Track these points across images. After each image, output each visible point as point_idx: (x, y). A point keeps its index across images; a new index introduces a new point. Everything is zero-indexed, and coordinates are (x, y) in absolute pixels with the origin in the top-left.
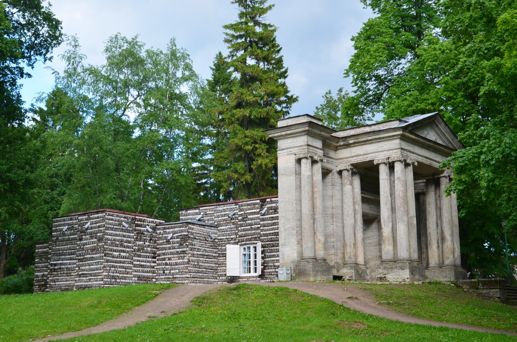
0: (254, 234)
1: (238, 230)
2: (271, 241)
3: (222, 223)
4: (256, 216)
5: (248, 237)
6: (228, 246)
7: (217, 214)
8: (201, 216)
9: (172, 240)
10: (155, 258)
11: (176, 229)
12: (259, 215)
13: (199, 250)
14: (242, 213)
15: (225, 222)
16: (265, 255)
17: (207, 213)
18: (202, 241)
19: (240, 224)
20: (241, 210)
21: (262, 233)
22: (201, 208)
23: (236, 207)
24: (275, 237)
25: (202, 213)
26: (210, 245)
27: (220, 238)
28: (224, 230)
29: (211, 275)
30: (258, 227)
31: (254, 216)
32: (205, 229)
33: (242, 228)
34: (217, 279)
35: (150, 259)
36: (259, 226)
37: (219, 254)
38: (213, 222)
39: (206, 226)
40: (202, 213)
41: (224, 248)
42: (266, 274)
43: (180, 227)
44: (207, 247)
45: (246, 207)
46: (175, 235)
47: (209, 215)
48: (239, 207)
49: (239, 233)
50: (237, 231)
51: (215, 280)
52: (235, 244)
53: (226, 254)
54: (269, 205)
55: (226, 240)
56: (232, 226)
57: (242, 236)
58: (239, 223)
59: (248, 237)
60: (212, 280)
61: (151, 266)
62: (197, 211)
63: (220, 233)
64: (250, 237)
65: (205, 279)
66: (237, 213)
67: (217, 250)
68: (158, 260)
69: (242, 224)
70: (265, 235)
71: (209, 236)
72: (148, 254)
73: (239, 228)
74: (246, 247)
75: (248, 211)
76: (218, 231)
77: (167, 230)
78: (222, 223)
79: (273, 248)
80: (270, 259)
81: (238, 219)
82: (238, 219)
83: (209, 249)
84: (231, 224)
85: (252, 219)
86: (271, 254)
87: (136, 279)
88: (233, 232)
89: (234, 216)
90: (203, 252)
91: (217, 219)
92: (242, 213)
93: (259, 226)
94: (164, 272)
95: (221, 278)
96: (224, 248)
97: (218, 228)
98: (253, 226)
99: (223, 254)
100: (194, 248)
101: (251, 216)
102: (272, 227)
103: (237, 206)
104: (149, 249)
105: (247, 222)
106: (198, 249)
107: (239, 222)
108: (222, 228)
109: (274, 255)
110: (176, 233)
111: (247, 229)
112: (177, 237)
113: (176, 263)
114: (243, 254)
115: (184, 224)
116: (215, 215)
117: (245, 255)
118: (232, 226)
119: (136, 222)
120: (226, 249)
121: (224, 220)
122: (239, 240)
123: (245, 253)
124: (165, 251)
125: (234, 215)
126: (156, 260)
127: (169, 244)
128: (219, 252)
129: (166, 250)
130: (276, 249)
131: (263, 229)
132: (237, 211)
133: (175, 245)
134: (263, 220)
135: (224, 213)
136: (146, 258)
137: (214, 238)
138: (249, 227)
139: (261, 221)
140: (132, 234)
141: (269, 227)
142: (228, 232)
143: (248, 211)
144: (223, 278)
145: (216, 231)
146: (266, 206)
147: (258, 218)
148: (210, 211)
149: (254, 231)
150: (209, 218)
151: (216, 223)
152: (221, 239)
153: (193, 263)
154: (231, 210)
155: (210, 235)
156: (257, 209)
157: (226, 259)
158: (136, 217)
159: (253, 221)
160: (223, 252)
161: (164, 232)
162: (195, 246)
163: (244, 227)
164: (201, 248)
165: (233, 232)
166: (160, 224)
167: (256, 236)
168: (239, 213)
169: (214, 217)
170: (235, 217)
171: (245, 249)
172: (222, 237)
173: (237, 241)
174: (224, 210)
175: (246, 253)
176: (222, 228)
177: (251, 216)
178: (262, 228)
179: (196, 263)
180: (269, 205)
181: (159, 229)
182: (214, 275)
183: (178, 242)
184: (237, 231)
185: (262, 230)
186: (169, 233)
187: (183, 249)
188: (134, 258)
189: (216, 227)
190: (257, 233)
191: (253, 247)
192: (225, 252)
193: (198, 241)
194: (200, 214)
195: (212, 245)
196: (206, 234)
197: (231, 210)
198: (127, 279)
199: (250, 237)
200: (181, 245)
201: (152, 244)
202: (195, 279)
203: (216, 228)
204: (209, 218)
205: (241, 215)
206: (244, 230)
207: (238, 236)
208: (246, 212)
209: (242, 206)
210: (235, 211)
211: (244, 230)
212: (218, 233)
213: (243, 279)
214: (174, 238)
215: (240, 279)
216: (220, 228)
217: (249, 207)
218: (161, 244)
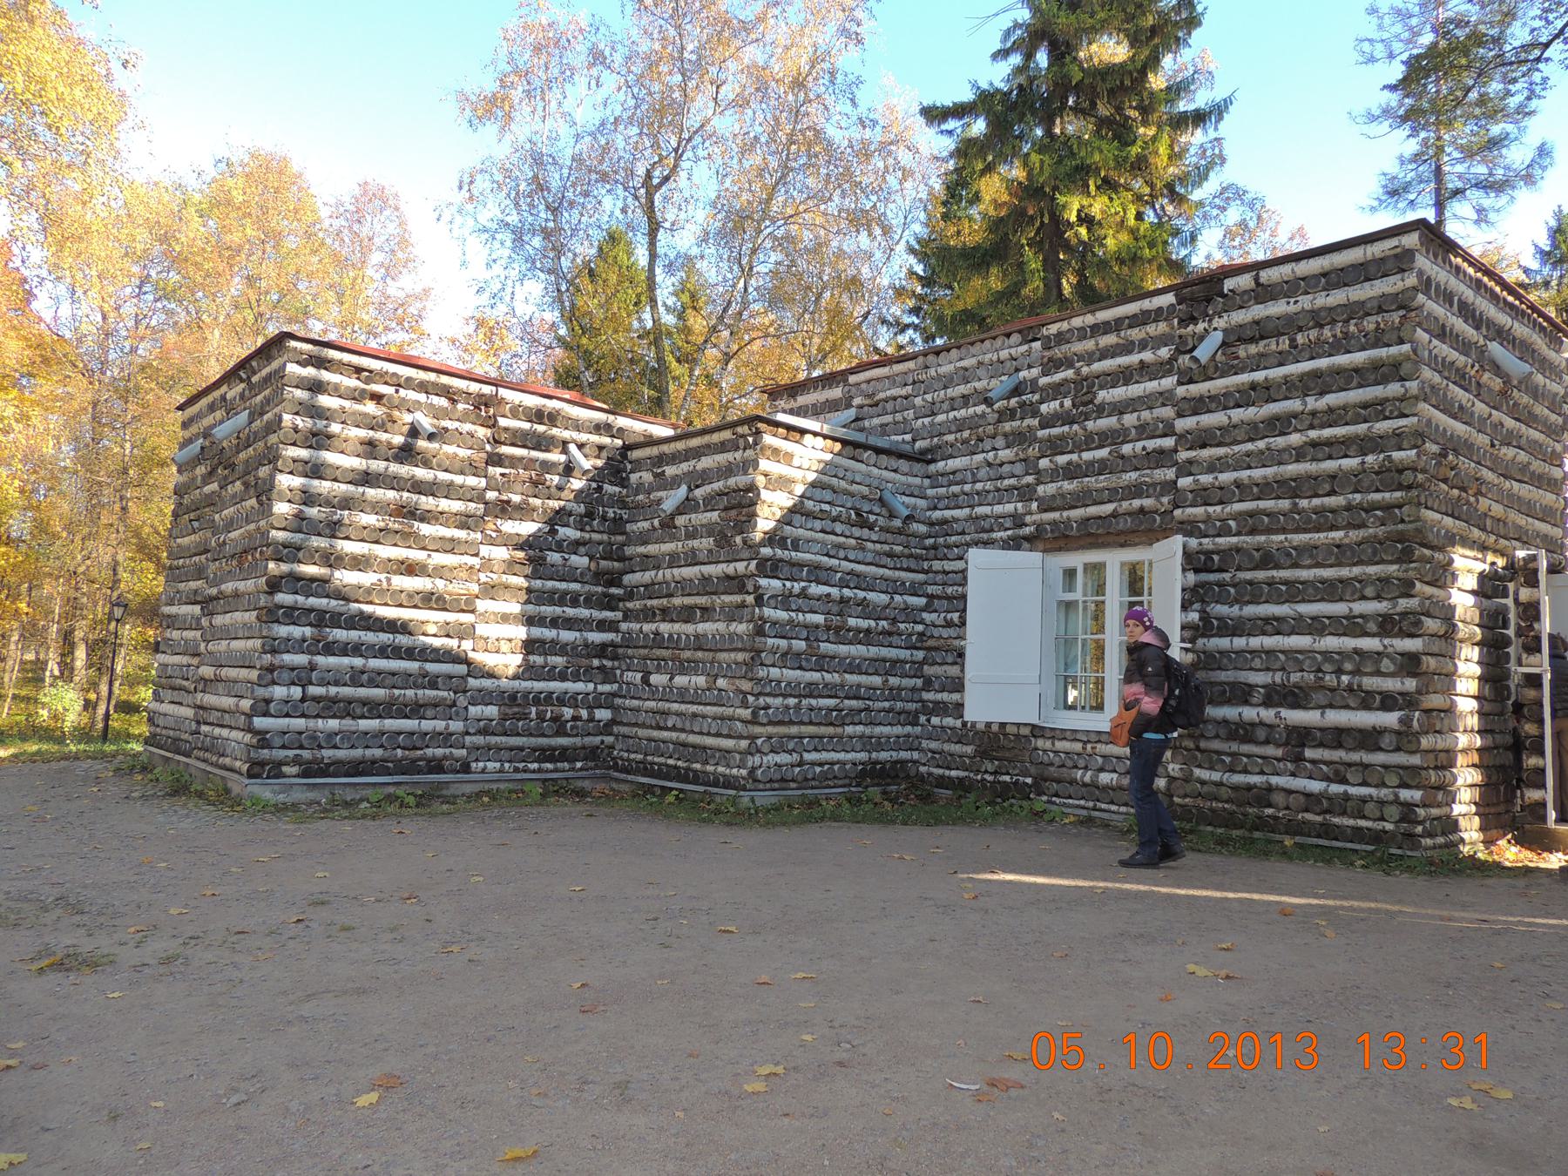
0: (1136, 491)
1: (1038, 472)
2: (1253, 532)
3: (950, 438)
4: (1152, 386)
5: (1093, 510)
6: (975, 555)
7: (929, 397)
8: (852, 412)
9: (680, 521)
10: (609, 603)
11: (706, 462)
12: (1168, 382)
13: (817, 573)
14: (1058, 377)
15: (966, 434)
16: (1205, 616)
17: (882, 395)
18: (839, 528)
19: (1049, 439)
20: (1051, 365)
21: (1185, 482)
22: (852, 379)
23: (1029, 351)
24: (1285, 504)
25: (857, 401)
26: (886, 548)
27: (937, 514)
28: (959, 477)
29: (887, 704)
30: (1161, 452)
31: (1135, 390)
32: (862, 467)
33: (1062, 459)
34: (915, 723)
35: (584, 613)
36: (1169, 442)
37: (931, 597)
38: (908, 437)
39: (866, 447)
40: (857, 401)
41: (959, 565)
42: (1210, 730)
43: (723, 447)
44: (869, 557)
45: (1089, 345)
46: (699, 493)
47: (889, 406)
48: (1047, 347)
49: (1041, 489)
50: (1030, 479)
51: (909, 729)
52: (1018, 548)
53: (964, 597)
54: (1239, 317)
55: (970, 527)
56: (1005, 454)
57: (1059, 502)
58: (1041, 434)
59: (1093, 510)
60: (886, 730)
61: (586, 645)
62: (836, 393)
63: (942, 491)
64: (1109, 508)
65: (849, 729)
66: (1034, 381)
67: (921, 577)
68: (626, 618)
69: (1062, 437)
70: (1203, 496)
71: (882, 501)
72: (575, 586)
73: (1044, 463)
74: (1077, 560)
75: (1098, 367)
76: (927, 482)
77: (670, 471)
78: (950, 438)
79: (1261, 575)
80: (1240, 642)
81: (1035, 413)
82: (1035, 413)
83: (881, 571)
84: (1000, 442)
85: (1120, 409)
86: (1251, 610)
87: (492, 711)
88: (1007, 482)
89: (1013, 401)
90: (843, 584)
91: (926, 420)
92: (1058, 377)
93: (1169, 442)
94: (646, 681)
95: (935, 720)
96: (959, 565)
97: (932, 468)
98: (1127, 449)
99: (949, 598)
100: (792, 564)
101: (1119, 393)
102: (1261, 444)
103: (1037, 345)
104: (579, 561)
105: (1090, 425)
106: (817, 567)
107: (1043, 427)
108: (953, 464)
109: (1267, 620)
110: (704, 477)
111: (1091, 463)
112: (709, 503)
113: (697, 636)
114: (1060, 603)
115: (740, 430)
116: (918, 401)
117: (1069, 606)
118: (1005, 454)
119: (503, 422)
120: (964, 571)
121: (960, 425)
122: (1039, 526)
123: (1069, 597)
124: (653, 573)
125: (1017, 391)
126: (619, 615)
127: (673, 538)
128: (930, 589)
129: (658, 568)
130: (1286, 582)
131: (1190, 462)
132: (1035, 372)
133: (695, 543)
134: (1199, 405)
135: (962, 389)
136: (561, 603)
137: (906, 512)
138: (1103, 453)
139: (1180, 415)
140: (472, 481)
141: (1236, 448)
142: (979, 486)
143: (1098, 367)
144: (949, 721)
145: (917, 481)
146: (1219, 323)
147: (1165, 398)
148: (894, 384)
149: (1133, 476)
150: (888, 419)
151: (919, 444)
152: (945, 522)
153: (783, 643)
154: (997, 368)
155: (887, 496)
156: (1155, 348)
157: (963, 623)
158: (503, 392)
159: (1130, 419)
160: (949, 590)
161: (656, 476)
162: (796, 548)
163: (1074, 457)
164: (834, 562)
165: (1007, 482)
166: (651, 441)
167: (1148, 502)
168: (1043, 381)
169: (910, 414)
170: (1022, 405)
171: (1070, 574)
172: (948, 514)
173: (1027, 530)
174: (965, 376)
175: (1077, 595)
176: (953, 464)
177: (1119, 393)
178: (1183, 455)
179: (800, 645)
180: (1239, 317)
181: (638, 465)
182: (899, 705)
183: (710, 529)
184: (1030, 479)
185: (1186, 469)
186: (675, 483)
187: (730, 569)
188: (481, 605)
189: (926, 458)
190: (1154, 485)
191: (1123, 564)
192: (953, 671)
193: (818, 524)
194: (849, 406)
195: (898, 549)
196: (865, 490)
197: (997, 368)
198: (429, 713)
199: (1109, 508)
200: (723, 540)
201: (596, 536)
202: (794, 730)
203: (917, 467)
204: (888, 419)
205: (1056, 391)
206: (1071, 472)
207: (1035, 505)
208: (1085, 370)
209: (1061, 338)
210: (1023, 374)
211: (1071, 472)
212: (930, 492)
213: (1060, 745)
214: (695, 509)
215: (1040, 743)
216: (941, 464)
217: (1109, 340)
218: (644, 539)
